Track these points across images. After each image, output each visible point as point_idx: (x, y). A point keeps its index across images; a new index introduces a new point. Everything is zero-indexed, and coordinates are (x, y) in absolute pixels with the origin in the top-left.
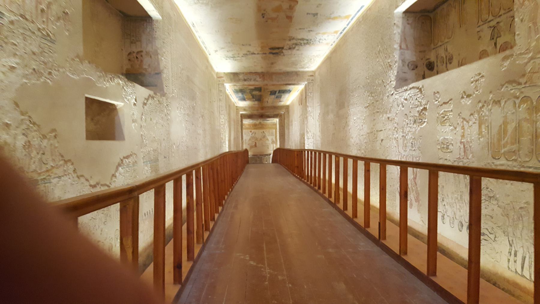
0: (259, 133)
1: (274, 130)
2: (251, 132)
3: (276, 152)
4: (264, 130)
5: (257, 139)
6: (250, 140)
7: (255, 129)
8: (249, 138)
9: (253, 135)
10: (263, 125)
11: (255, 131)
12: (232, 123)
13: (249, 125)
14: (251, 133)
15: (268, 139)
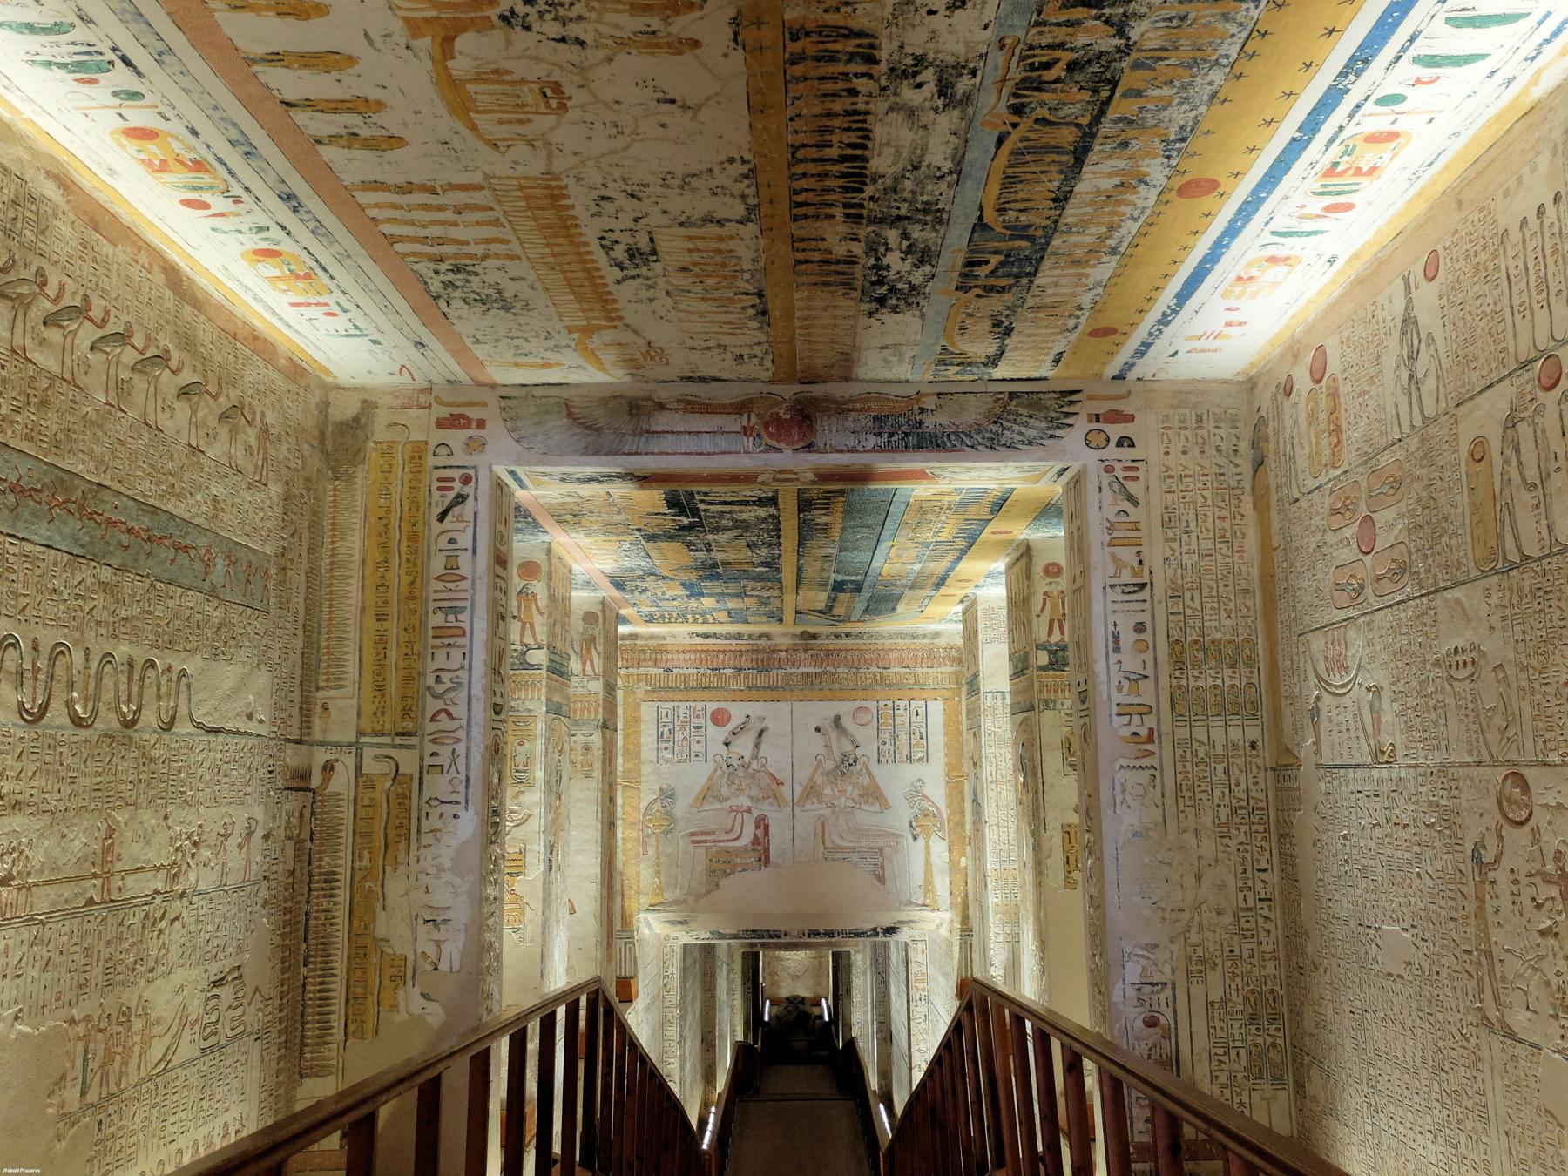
0: (792, 732)
1: (936, 709)
2: (719, 718)
4: (845, 708)
6: (708, 794)
7: (754, 692)
8: (697, 775)
9: (744, 746)
10: (829, 655)
11: (755, 709)
14: (717, 734)
15: (873, 794)
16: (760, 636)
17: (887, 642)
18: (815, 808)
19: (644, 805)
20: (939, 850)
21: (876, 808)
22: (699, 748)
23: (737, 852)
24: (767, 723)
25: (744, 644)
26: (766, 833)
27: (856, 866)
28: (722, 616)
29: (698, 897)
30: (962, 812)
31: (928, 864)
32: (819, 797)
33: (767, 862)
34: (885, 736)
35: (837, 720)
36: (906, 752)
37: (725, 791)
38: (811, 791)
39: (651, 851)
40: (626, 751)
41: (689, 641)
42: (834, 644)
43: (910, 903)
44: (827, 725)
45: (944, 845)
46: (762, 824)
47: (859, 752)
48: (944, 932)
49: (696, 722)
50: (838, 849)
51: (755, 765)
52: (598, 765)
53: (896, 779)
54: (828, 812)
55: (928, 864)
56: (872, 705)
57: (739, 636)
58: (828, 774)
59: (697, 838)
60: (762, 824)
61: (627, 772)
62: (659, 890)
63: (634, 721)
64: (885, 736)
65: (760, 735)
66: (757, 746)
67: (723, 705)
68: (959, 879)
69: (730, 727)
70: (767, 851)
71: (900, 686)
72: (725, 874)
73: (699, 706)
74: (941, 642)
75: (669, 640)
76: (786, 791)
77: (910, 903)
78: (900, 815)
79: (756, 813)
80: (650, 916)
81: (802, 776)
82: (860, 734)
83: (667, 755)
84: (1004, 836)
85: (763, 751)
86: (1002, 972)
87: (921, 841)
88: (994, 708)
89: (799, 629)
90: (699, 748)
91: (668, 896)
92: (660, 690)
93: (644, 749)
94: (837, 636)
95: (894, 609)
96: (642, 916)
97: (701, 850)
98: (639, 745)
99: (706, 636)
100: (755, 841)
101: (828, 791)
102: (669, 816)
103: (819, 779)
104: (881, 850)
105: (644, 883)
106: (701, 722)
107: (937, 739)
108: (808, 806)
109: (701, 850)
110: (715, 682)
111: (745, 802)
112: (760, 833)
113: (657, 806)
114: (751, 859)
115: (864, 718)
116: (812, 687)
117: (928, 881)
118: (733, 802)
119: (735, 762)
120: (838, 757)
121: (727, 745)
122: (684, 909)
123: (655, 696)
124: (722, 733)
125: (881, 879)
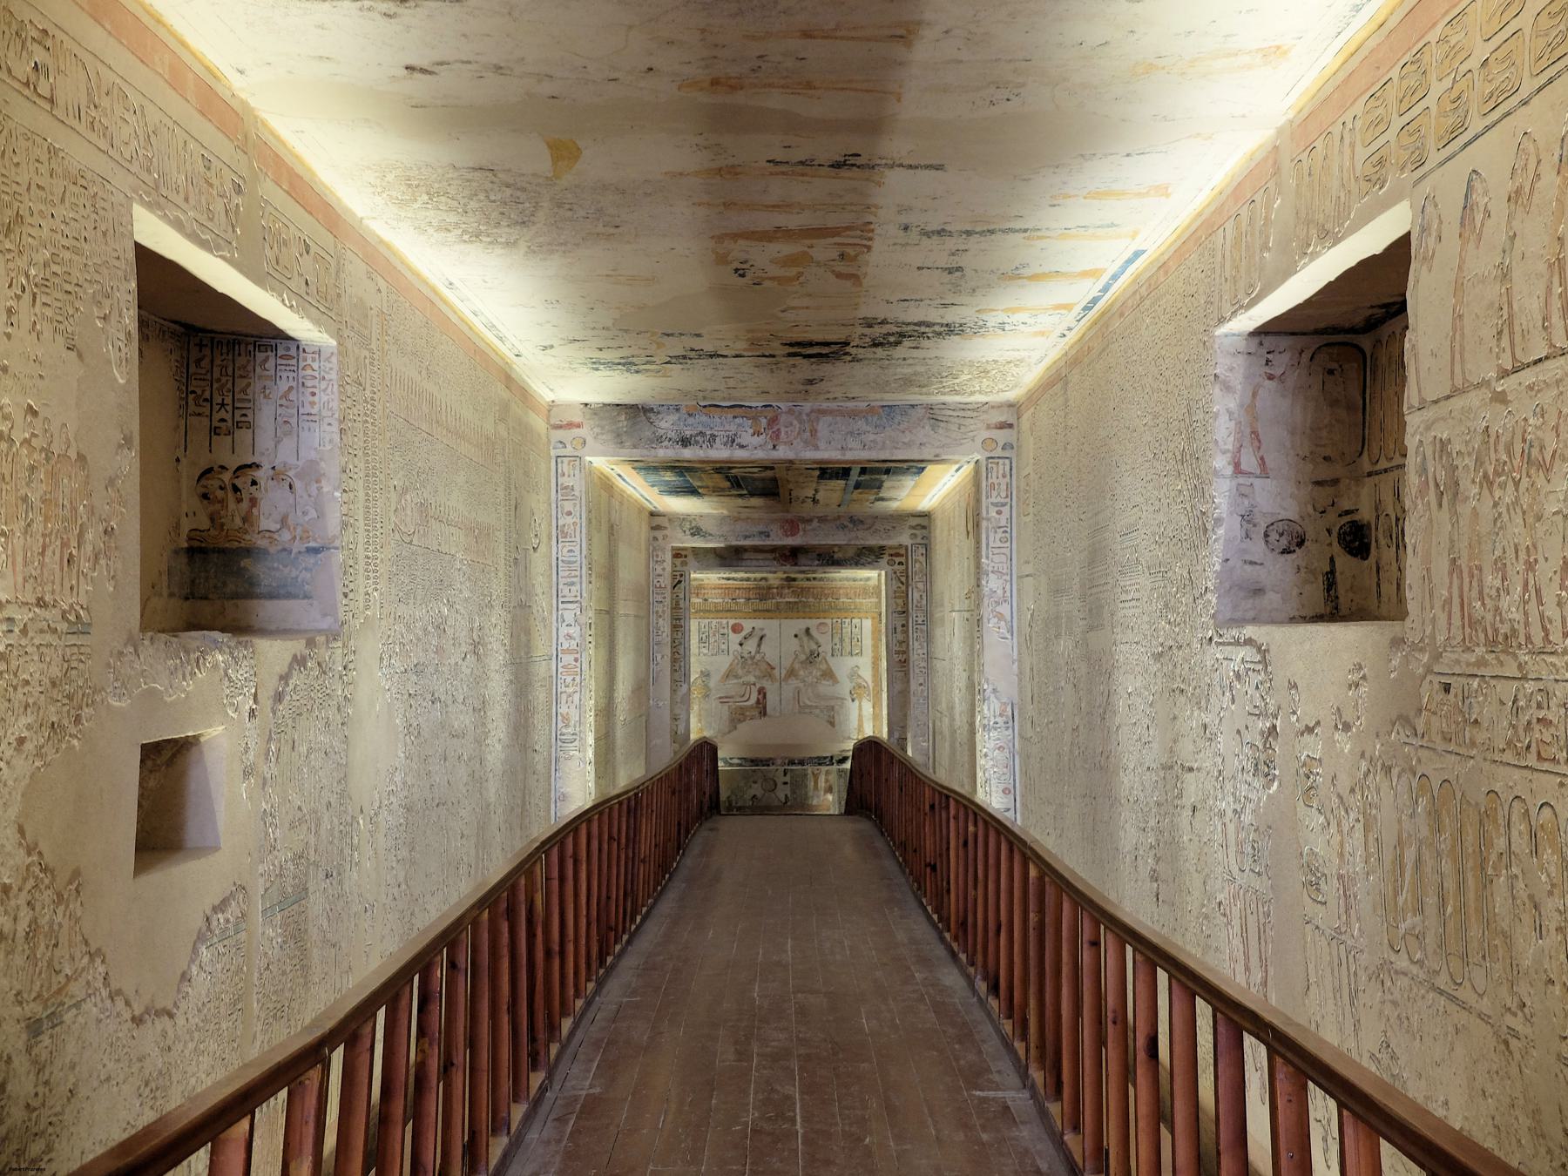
1: (868, 624)
2: (736, 629)
3: (869, 750)
4: (812, 623)
6: (730, 674)
8: (723, 663)
9: (751, 646)
10: (803, 591)
11: (758, 623)
12: (625, 608)
14: (735, 638)
15: (829, 675)
18: (794, 683)
20: (867, 707)
22: (724, 647)
23: (747, 708)
31: (860, 716)
34: (836, 640)
35: (807, 630)
37: (740, 672)
38: (792, 673)
42: (806, 584)
44: (802, 634)
46: (762, 692)
50: (807, 706)
53: (843, 666)
55: (860, 716)
56: (829, 621)
57: (748, 579)
59: (723, 700)
60: (762, 692)
64: (836, 640)
69: (743, 634)
71: (846, 610)
76: (776, 672)
78: (845, 687)
81: (786, 664)
90: (724, 647)
97: (726, 707)
100: (758, 702)
102: (706, 686)
103: (797, 666)
104: (833, 708)
107: (868, 642)
109: (726, 707)
110: (734, 607)
111: (752, 679)
114: (756, 713)
115: (823, 629)
116: (793, 610)
120: (807, 651)
125: (832, 724)
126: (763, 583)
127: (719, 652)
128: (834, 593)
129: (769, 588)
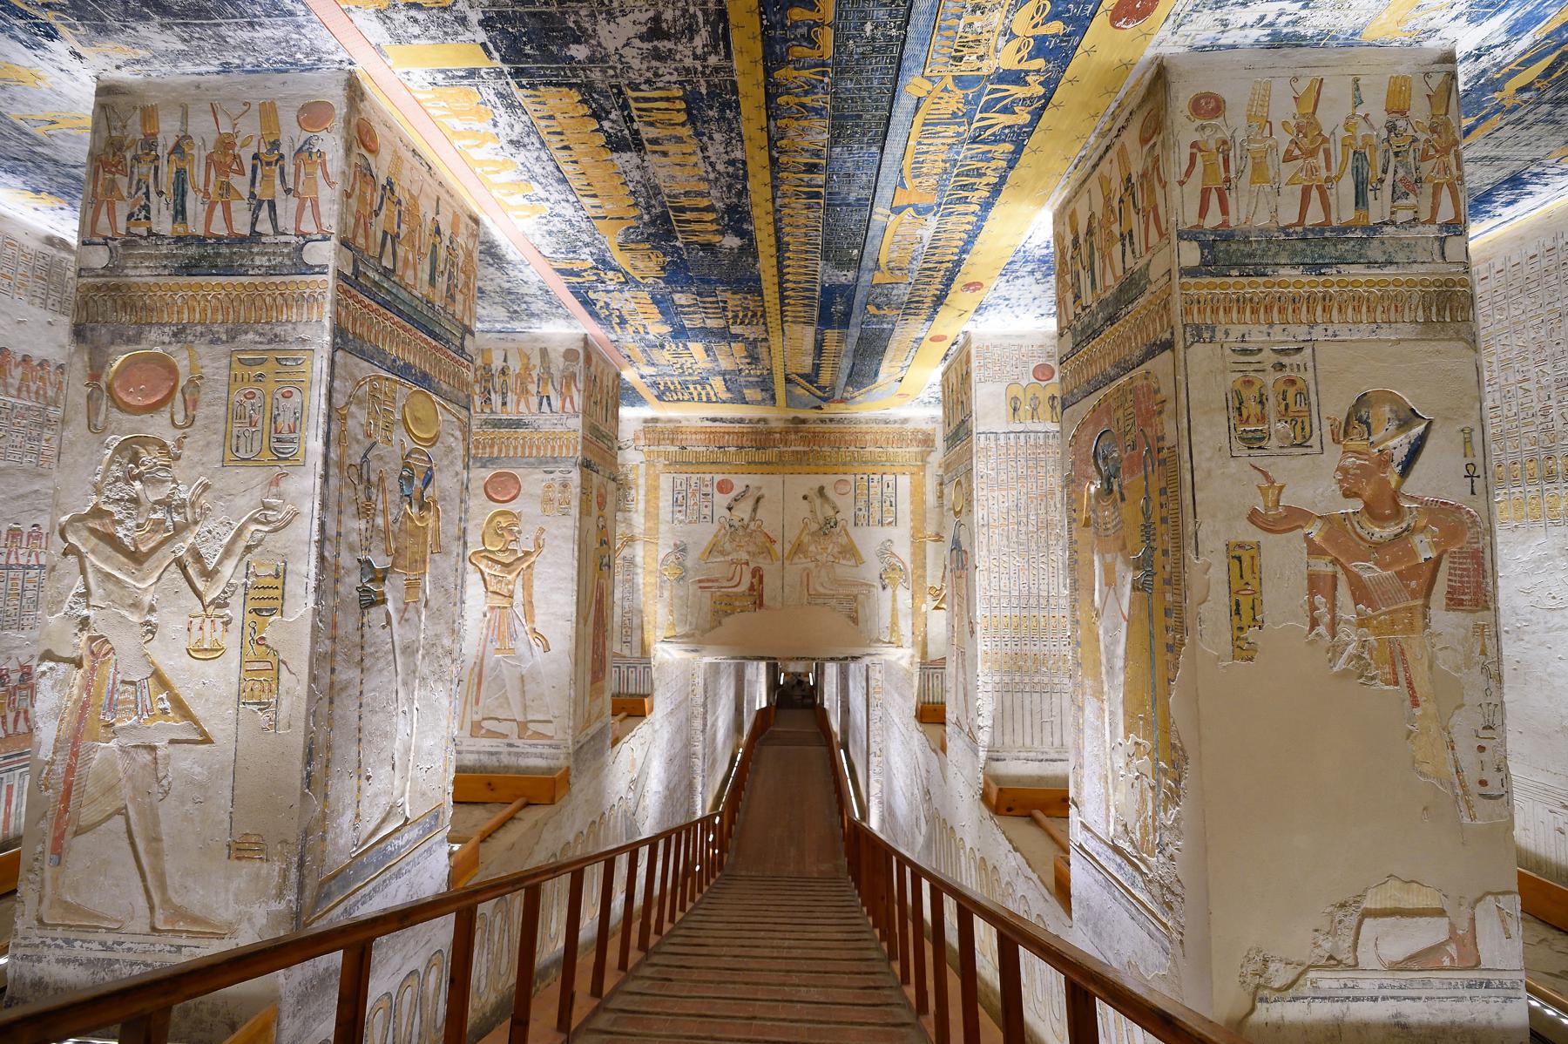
0: (786, 498)
1: (904, 482)
2: (724, 487)
4: (827, 480)
5: (767, 545)
6: (714, 549)
7: (753, 466)
8: (705, 533)
9: (743, 511)
10: (815, 438)
11: (754, 480)
13: (715, 435)
14: (722, 500)
15: (850, 551)
16: (759, 421)
17: (864, 427)
18: (802, 562)
19: (661, 556)
20: (904, 597)
21: (852, 562)
22: (707, 511)
23: (736, 595)
24: (763, 491)
25: (744, 427)
26: (761, 581)
27: (834, 609)
28: (718, 383)
29: (704, 632)
30: (924, 567)
32: (805, 553)
33: (761, 605)
34: (861, 504)
35: (821, 490)
36: (878, 516)
37: (728, 546)
38: (799, 548)
39: (666, 594)
40: (647, 513)
41: (700, 424)
43: (879, 641)
44: (813, 495)
45: (909, 594)
46: (757, 573)
47: (839, 517)
48: (905, 663)
49: (705, 490)
50: (820, 595)
51: (752, 526)
52: (575, 503)
53: (869, 540)
54: (812, 565)
56: (850, 478)
57: (741, 421)
58: (813, 534)
60: (757, 573)
61: (647, 531)
62: (673, 625)
63: (653, 489)
64: (861, 504)
65: (758, 500)
66: (755, 510)
67: (726, 476)
68: (920, 620)
69: (733, 494)
70: (761, 596)
71: (875, 463)
72: (727, 614)
73: (708, 477)
74: (909, 426)
75: (684, 423)
76: (777, 547)
77: (879, 641)
78: (872, 569)
79: (752, 565)
80: (665, 646)
81: (792, 535)
82: (840, 502)
83: (681, 517)
84: (994, 582)
85: (760, 513)
86: (990, 723)
87: (889, 590)
88: (987, 449)
89: (792, 413)
90: (707, 511)
91: (680, 630)
92: (676, 464)
93: (662, 512)
94: (823, 421)
95: (876, 374)
96: (658, 646)
98: (657, 507)
99: (714, 420)
100: (752, 588)
101: (812, 548)
103: (806, 539)
104: (855, 597)
105: (660, 619)
106: (709, 490)
107: (905, 506)
108: (796, 560)
111: (745, 556)
112: (755, 581)
113: (672, 558)
114: (748, 603)
115: (842, 488)
117: (894, 623)
118: (734, 556)
119: (737, 524)
120: (822, 521)
121: (730, 509)
122: (697, 637)
123: (672, 469)
124: (726, 499)
125: (855, 620)
126: (761, 426)
127: (701, 518)
128: (858, 440)
129: (770, 432)
